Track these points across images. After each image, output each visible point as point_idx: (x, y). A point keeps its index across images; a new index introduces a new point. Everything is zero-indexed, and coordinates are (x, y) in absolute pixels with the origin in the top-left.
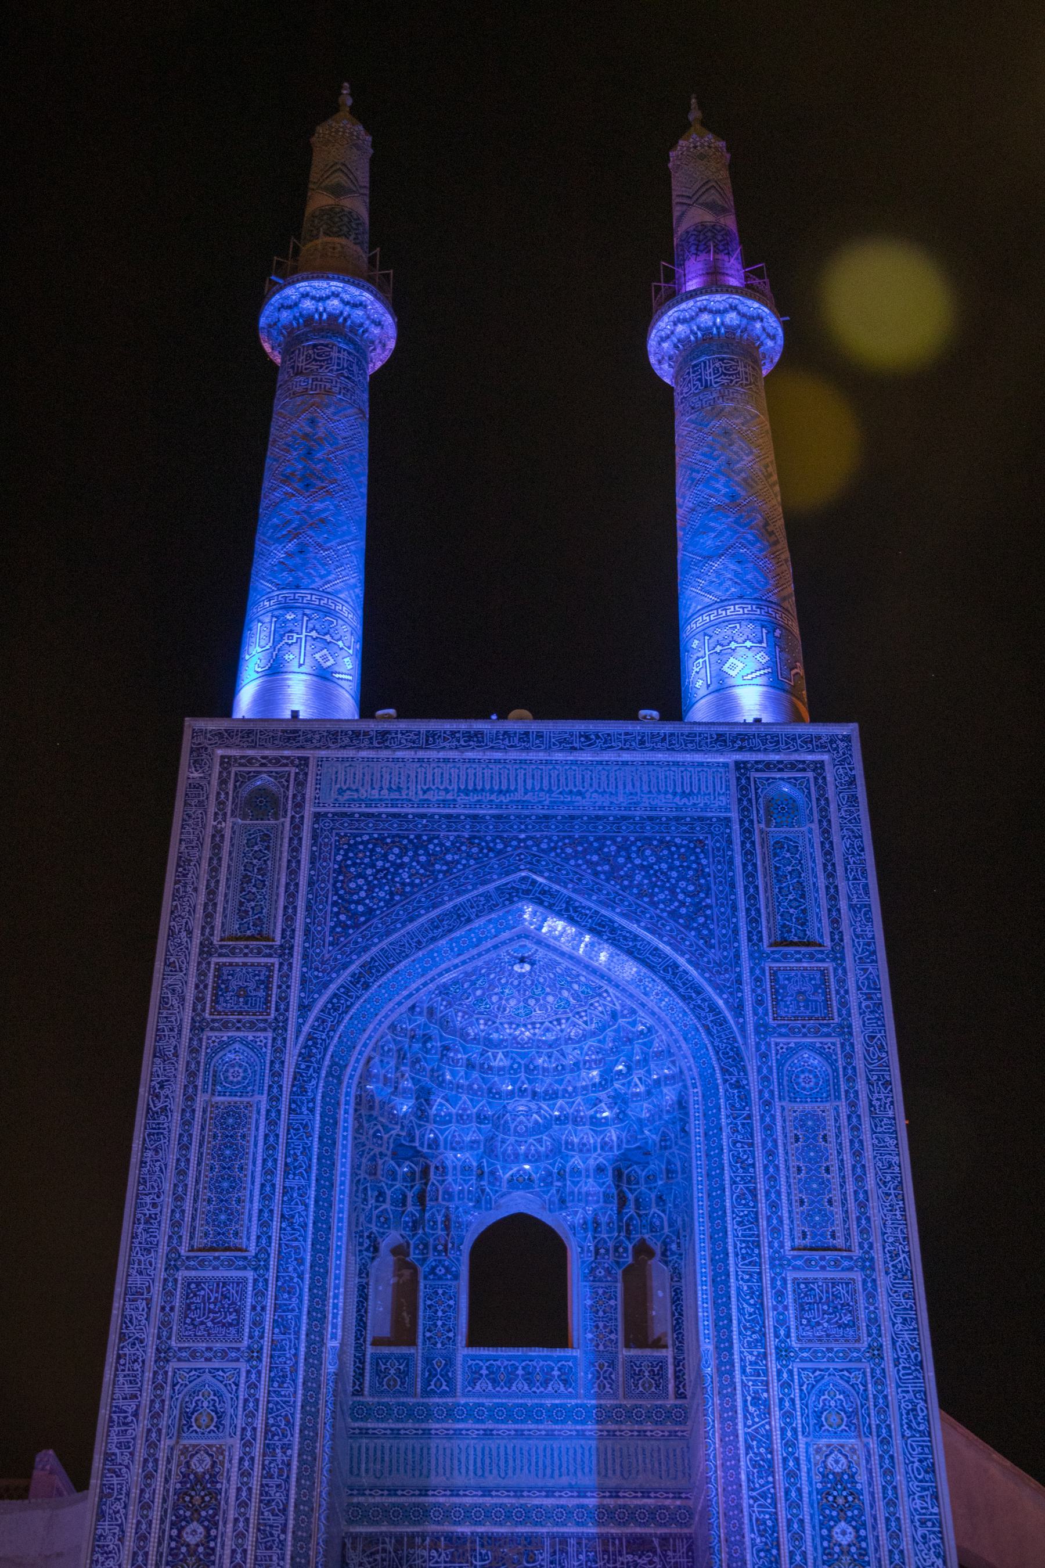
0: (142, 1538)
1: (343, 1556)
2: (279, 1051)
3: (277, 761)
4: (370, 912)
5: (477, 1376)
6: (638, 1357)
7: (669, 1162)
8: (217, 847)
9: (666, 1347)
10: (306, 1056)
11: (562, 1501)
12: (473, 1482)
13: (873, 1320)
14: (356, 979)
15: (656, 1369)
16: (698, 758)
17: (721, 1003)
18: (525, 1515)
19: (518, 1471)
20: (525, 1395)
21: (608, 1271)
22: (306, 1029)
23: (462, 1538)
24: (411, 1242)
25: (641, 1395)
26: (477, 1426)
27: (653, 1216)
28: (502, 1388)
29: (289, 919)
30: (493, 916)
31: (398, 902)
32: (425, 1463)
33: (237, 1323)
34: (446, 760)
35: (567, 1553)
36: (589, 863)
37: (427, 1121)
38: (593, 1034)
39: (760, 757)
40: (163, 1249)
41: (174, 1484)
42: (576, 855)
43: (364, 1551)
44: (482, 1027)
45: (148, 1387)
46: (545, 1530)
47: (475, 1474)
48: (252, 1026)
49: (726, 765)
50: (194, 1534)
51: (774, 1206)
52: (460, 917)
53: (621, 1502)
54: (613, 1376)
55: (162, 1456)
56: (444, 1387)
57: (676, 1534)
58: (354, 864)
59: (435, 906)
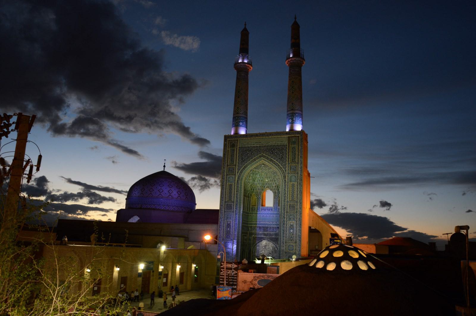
0: (224, 230)
2: (235, 178)
3: (235, 140)
4: (245, 160)
8: (228, 152)
10: (238, 178)
13: (297, 209)
14: (243, 168)
16: (284, 136)
17: (284, 170)
18: (267, 224)
21: (277, 197)
22: (238, 175)
29: (236, 161)
30: (258, 160)
33: (232, 209)
34: (254, 139)
36: (269, 152)
39: (291, 136)
40: (224, 201)
41: (226, 224)
42: (268, 151)
45: (223, 215)
46: (269, 226)
48: (232, 175)
49: (287, 137)
50: (228, 229)
51: (287, 195)
52: (255, 160)
55: (225, 222)
59: (252, 159)
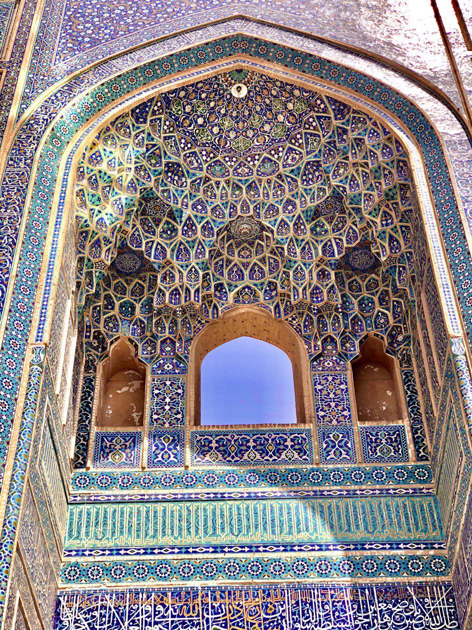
1: (57, 614)
5: (207, 448)
6: (373, 428)
7: (391, 237)
9: (400, 418)
11: (302, 555)
12: (204, 541)
15: (393, 437)
19: (252, 529)
20: (258, 462)
23: (192, 593)
24: (140, 346)
25: (380, 459)
26: (207, 491)
27: (378, 315)
28: (233, 457)
31: (122, 35)
32: (151, 525)
35: (311, 604)
37: (154, 234)
38: (308, 153)
43: (80, 609)
44: (204, 158)
47: (206, 532)
53: (368, 553)
54: (349, 445)
56: (172, 458)
57: (432, 583)
58: (83, 16)
